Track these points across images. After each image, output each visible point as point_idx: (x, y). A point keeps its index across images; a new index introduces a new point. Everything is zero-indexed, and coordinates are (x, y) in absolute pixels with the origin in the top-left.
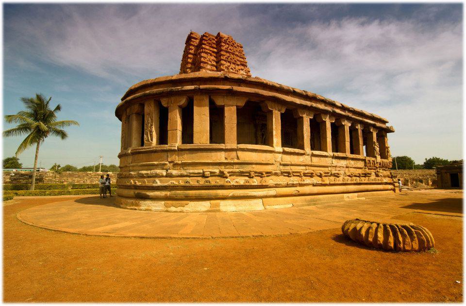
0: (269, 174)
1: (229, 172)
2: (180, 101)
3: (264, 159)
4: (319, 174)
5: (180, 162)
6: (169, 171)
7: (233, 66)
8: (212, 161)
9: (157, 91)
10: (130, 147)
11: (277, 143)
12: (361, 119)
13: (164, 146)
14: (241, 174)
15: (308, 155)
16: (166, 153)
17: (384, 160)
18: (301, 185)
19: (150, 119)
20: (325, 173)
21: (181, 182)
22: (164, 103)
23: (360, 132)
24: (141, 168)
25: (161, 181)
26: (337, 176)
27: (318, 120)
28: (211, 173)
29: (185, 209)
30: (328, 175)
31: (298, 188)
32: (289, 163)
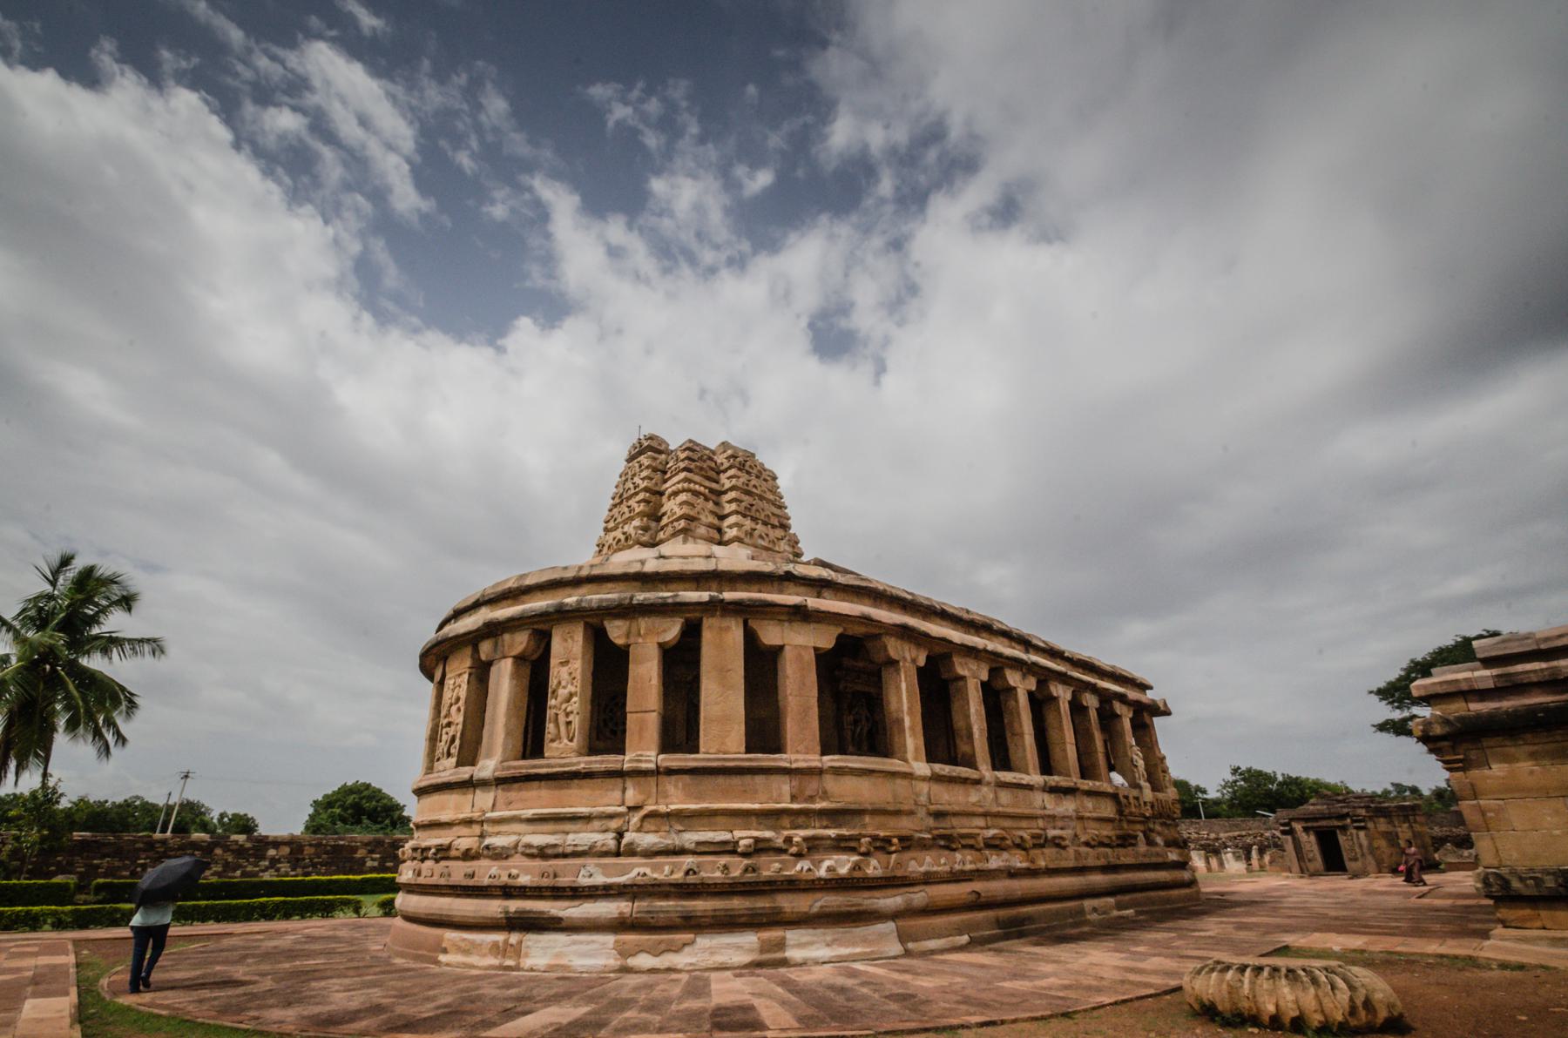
0: (907, 843)
1: (806, 839)
3: (890, 799)
4: (1018, 841)
5: (662, 808)
6: (628, 837)
8: (757, 806)
9: (601, 600)
10: (489, 756)
11: (916, 749)
13: (612, 757)
15: (989, 784)
16: (619, 781)
17: (1160, 795)
20: (1034, 837)
21: (668, 871)
22: (617, 631)
23: (1093, 714)
24: (531, 828)
25: (606, 870)
26: (1057, 843)
27: (998, 685)
28: (757, 840)
29: (681, 960)
30: (1041, 842)
31: (978, 886)
32: (947, 808)
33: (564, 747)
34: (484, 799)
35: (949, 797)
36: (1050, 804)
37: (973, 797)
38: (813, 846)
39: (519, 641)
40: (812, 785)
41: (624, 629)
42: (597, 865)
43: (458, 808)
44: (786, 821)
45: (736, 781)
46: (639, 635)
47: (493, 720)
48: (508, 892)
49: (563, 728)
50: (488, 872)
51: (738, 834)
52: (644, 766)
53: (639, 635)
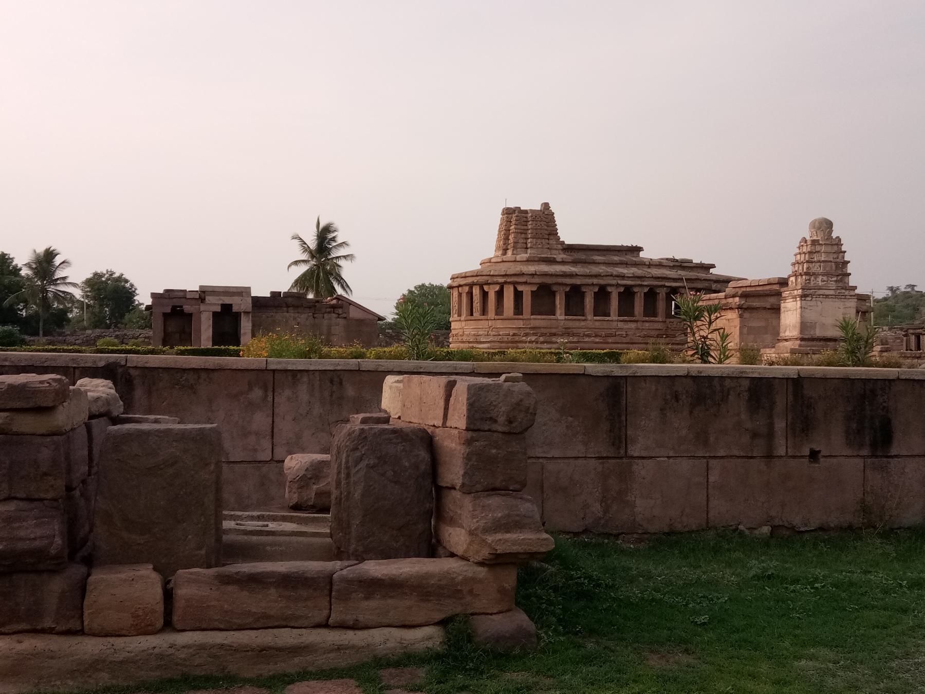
7: (539, 241)
12: (662, 283)
14: (534, 334)
18: (578, 342)
21: (496, 339)
22: (486, 288)
33: (476, 314)
34: (463, 324)
35: (571, 324)
36: (620, 325)
37: (583, 323)
38: (526, 335)
39: (467, 289)
40: (528, 322)
48: (469, 342)
50: (465, 338)
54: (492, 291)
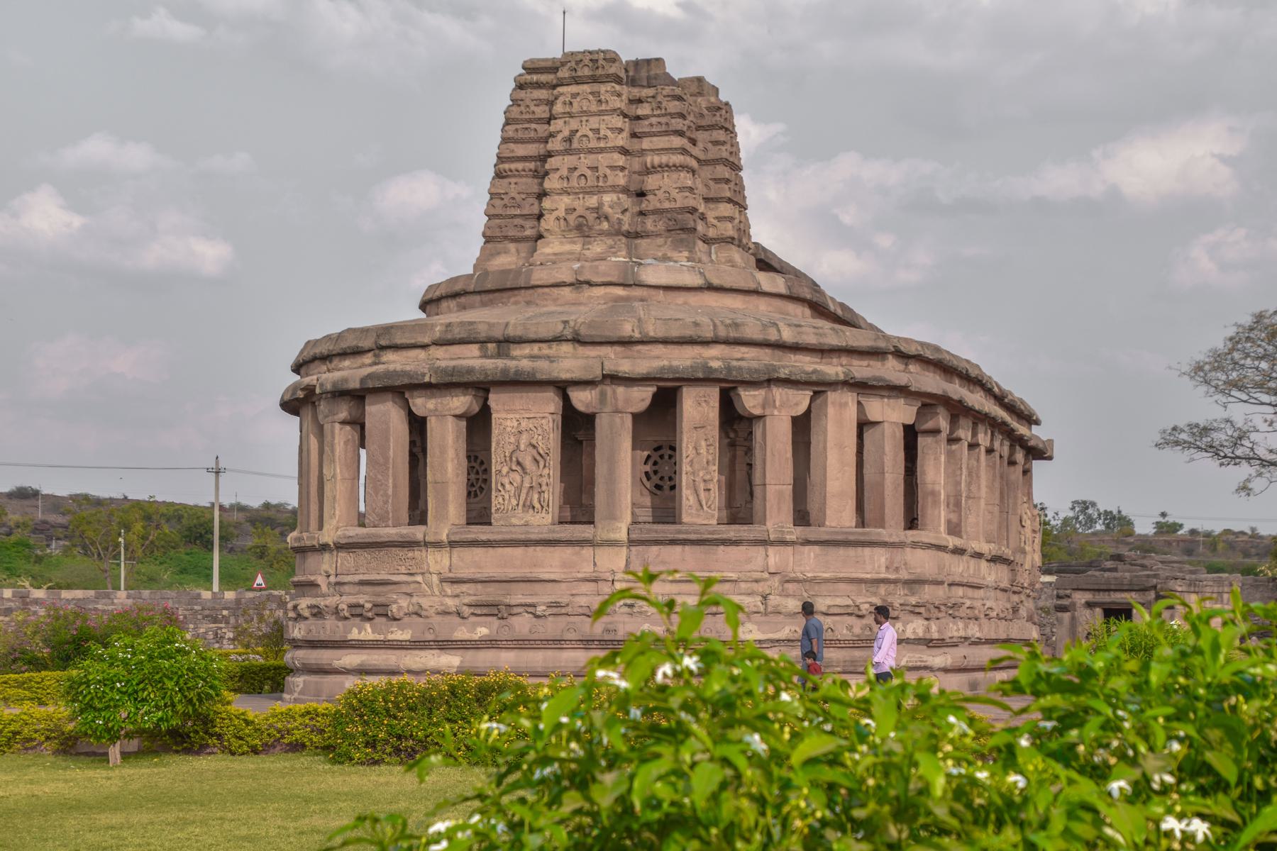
2: (797, 404)
6: (774, 600)
8: (869, 576)
10: (613, 517)
16: (761, 549)
19: (703, 443)
22: (750, 400)
39: (641, 397)
41: (760, 400)
42: (757, 623)
43: (564, 565)
44: (882, 589)
45: (851, 552)
46: (775, 407)
47: (612, 479)
49: (702, 495)
51: (859, 600)
52: (788, 538)
53: (775, 407)
54: (776, 411)
